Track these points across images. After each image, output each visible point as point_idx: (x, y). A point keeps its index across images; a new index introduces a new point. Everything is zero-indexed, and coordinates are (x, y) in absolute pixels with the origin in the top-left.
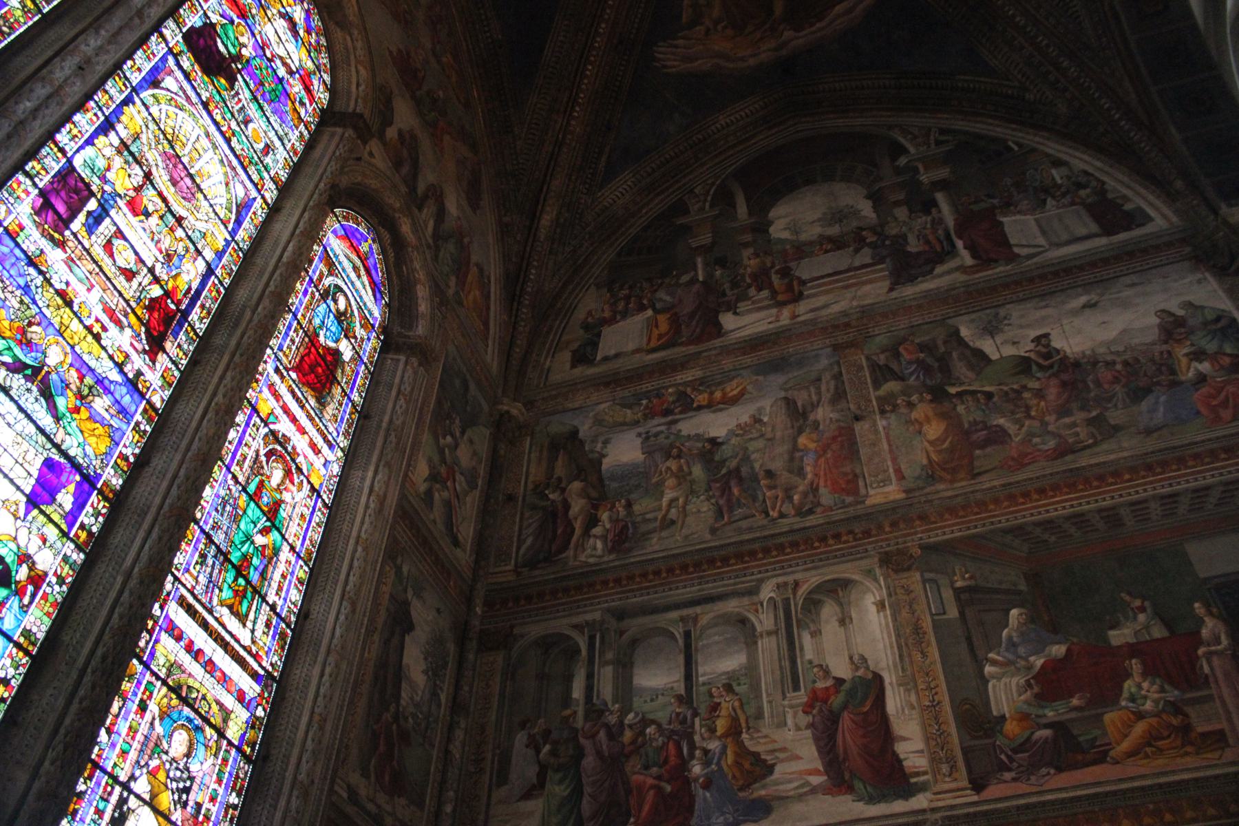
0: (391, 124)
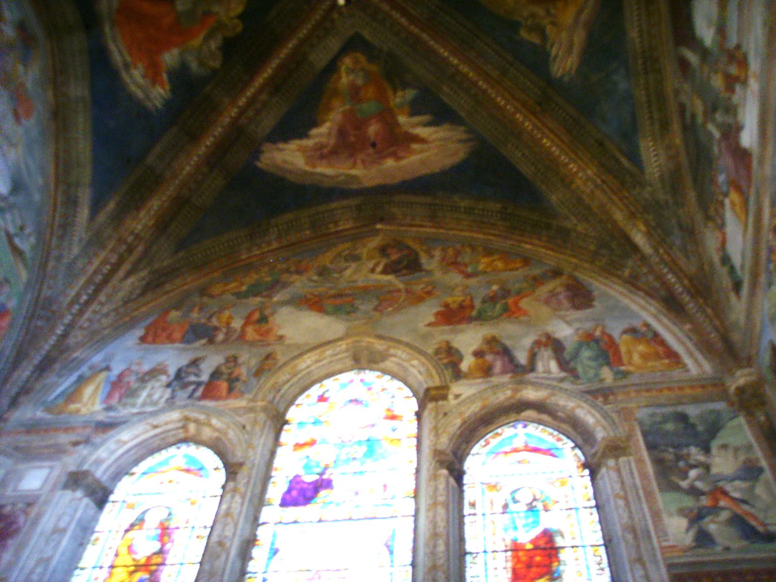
0: (461, 359)
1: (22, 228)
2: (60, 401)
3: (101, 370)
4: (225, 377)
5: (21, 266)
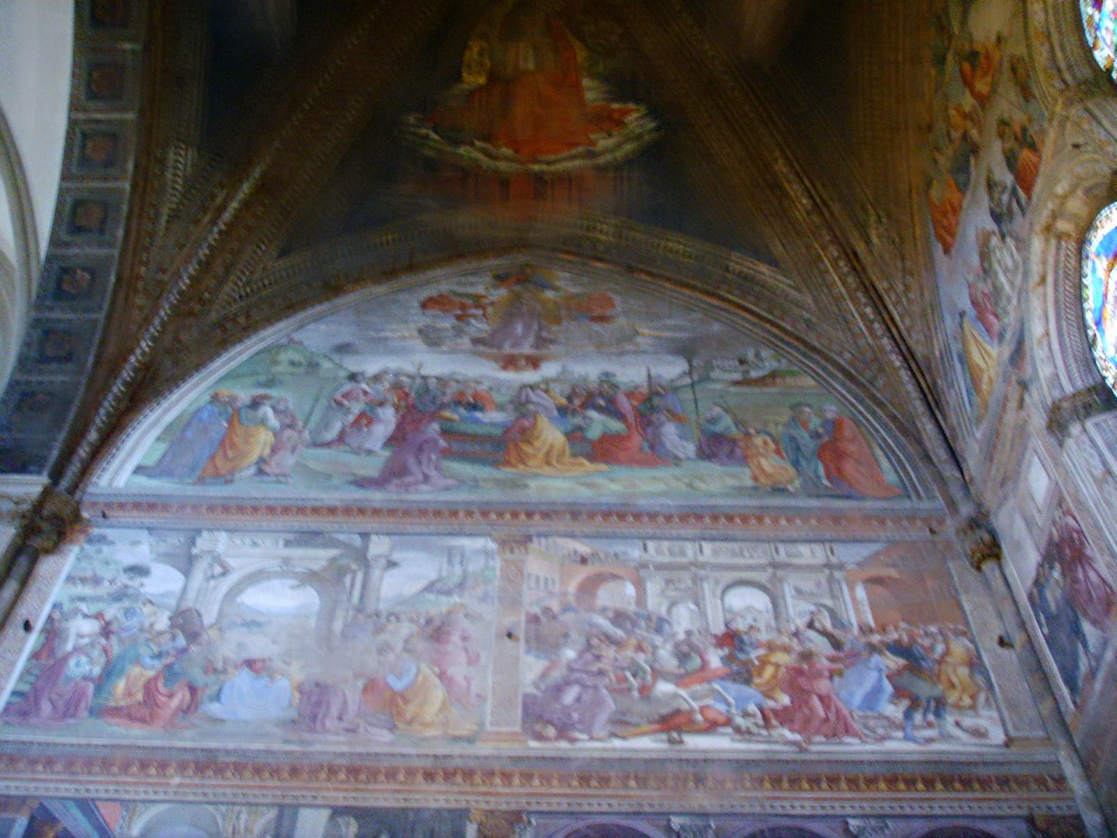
1: (742, 362)
2: (976, 399)
3: (962, 328)
4: (1016, 147)
5: (790, 380)
